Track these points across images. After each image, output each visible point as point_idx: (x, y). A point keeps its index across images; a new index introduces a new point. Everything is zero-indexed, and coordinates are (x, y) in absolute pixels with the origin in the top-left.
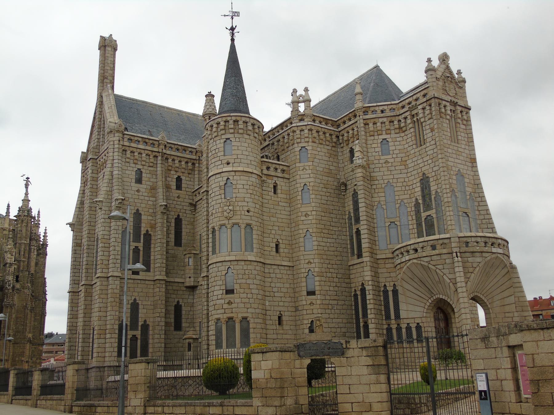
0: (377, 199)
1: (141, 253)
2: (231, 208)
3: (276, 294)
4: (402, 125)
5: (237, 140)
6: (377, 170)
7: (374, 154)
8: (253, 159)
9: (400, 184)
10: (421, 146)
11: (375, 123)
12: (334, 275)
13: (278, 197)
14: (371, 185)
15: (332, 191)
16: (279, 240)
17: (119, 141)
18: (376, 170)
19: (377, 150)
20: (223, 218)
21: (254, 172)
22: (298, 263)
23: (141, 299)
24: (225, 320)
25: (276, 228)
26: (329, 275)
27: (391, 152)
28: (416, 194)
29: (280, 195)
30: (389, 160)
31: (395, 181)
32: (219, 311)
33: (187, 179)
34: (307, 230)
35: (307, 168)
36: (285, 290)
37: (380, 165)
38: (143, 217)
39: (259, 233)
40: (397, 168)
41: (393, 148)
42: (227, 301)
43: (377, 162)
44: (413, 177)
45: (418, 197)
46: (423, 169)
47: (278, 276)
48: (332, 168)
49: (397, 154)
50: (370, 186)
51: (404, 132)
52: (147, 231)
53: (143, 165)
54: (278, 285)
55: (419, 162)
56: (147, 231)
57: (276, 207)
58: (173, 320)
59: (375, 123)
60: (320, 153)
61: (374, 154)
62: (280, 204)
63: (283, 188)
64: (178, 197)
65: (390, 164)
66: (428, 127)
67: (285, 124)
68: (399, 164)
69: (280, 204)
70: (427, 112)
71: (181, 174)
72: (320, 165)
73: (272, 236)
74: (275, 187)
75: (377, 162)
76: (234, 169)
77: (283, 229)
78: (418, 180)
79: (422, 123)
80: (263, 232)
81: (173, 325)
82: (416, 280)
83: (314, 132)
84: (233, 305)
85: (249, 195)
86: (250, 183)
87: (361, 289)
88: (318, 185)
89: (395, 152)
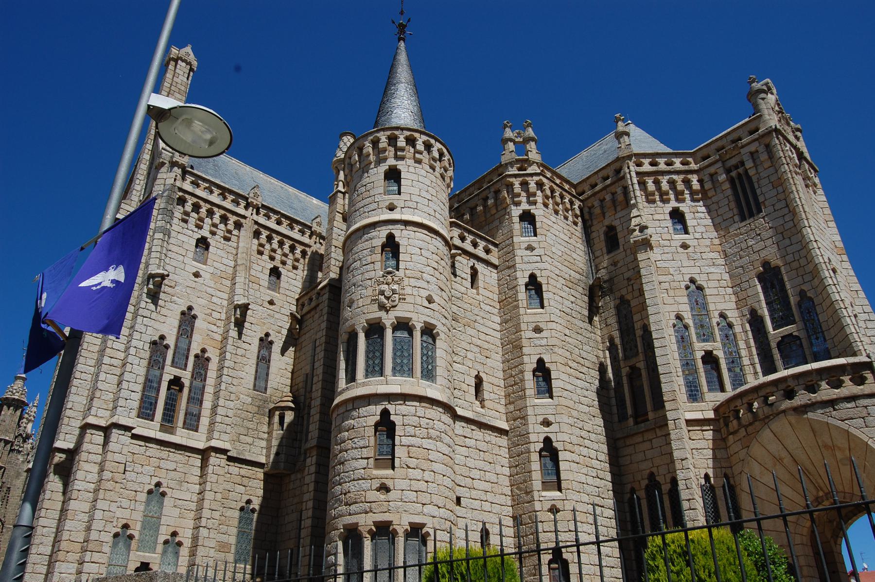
0: (675, 308)
1: (186, 391)
2: (395, 287)
3: (476, 484)
4: (708, 186)
5: (412, 169)
6: (669, 256)
8: (438, 209)
10: (751, 215)
11: (657, 183)
12: (593, 454)
13: (478, 294)
15: (578, 295)
16: (481, 374)
17: (175, 180)
18: (665, 257)
20: (375, 307)
22: (518, 422)
23: (172, 484)
24: (368, 528)
25: (477, 349)
26: (585, 451)
27: (690, 229)
28: (750, 302)
29: (481, 291)
30: (688, 242)
31: (704, 277)
32: (353, 508)
33: (290, 274)
34: (538, 356)
35: (535, 245)
36: (493, 478)
38: (198, 323)
41: (694, 223)
42: (376, 484)
43: (667, 243)
45: (756, 306)
46: (763, 254)
47: (482, 446)
48: (574, 256)
49: (702, 233)
51: (710, 198)
52: (204, 351)
53: (213, 233)
54: (481, 464)
55: (751, 242)
56: (204, 351)
58: (233, 540)
59: (657, 183)
60: (555, 226)
63: (488, 280)
64: (271, 303)
65: (690, 250)
66: (764, 182)
67: (487, 180)
70: (764, 157)
71: (277, 263)
72: (557, 245)
73: (470, 364)
74: (474, 274)
75: (667, 243)
76: (405, 217)
77: (488, 354)
79: (749, 178)
81: (233, 550)
82: (787, 460)
83: (547, 187)
84: (392, 495)
85: (432, 271)
86: (432, 248)
87: (647, 486)
88: (555, 277)
89: (698, 229)
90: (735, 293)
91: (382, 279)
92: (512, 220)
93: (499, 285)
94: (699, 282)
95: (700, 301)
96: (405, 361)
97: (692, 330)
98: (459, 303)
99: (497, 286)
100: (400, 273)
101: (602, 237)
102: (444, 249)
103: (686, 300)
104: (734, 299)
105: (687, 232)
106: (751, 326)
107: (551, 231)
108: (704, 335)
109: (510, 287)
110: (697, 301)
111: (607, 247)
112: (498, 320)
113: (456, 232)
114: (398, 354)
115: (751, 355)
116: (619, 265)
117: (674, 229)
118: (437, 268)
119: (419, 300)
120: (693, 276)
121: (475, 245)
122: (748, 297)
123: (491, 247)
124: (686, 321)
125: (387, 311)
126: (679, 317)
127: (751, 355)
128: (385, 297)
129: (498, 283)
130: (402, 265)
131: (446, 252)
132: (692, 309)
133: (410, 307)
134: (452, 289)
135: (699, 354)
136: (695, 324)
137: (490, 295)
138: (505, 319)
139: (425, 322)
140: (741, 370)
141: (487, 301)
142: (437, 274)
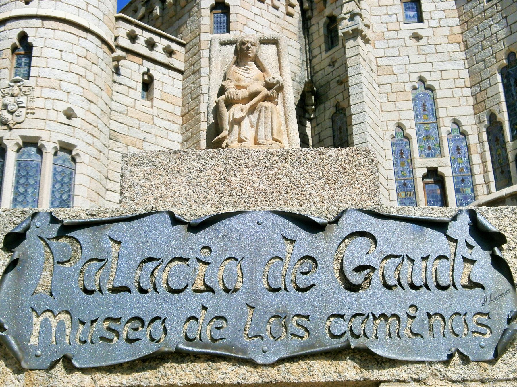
0: (395, 116)
2: (23, 99)
6: (395, 52)
7: (385, 18)
9: (451, 84)
14: (379, 85)
19: (392, 10)
21: (93, 28)
27: (425, 16)
28: (489, 104)
29: (156, 102)
30: (420, 32)
37: (401, 42)
39: (96, 175)
40: (440, 49)
44: (481, 65)
45: (495, 109)
49: (440, 20)
50: (376, 86)
57: (146, 127)
60: (258, 19)
61: (385, 18)
62: (157, 120)
63: (167, 88)
68: (446, 40)
69: (157, 120)
78: (495, 69)
80: (107, 178)
85: (74, 78)
89: (435, 15)
90: (474, 95)
91: (7, 90)
92: (201, 13)
93: (184, 95)
94: (429, 83)
95: (429, 106)
96: (30, 190)
97: (415, 143)
98: (121, 118)
99: (180, 96)
100: (31, 82)
101: (322, 31)
102: (102, 51)
103: (410, 105)
104: (471, 101)
105: (420, 20)
106: (488, 134)
107: (250, 26)
108: (429, 148)
109: (194, 96)
110: (424, 106)
111: (326, 43)
112: (179, 138)
113: (124, 28)
114: (22, 181)
115: (486, 172)
116: (337, 65)
117: (407, 16)
118: (83, 74)
119: (53, 115)
120: (422, 74)
121: (151, 45)
122: (488, 98)
123: (174, 46)
124: (408, 131)
125: (10, 129)
126: (400, 126)
127: (486, 172)
128: (10, 112)
129: (183, 93)
130: (34, 72)
131: (101, 54)
132: (417, 116)
133: (41, 124)
134: (112, 100)
135: (420, 172)
136: (419, 135)
137: (170, 108)
138: (186, 136)
139: (60, 142)
140: (473, 190)
141: (164, 115)
142: (84, 83)
